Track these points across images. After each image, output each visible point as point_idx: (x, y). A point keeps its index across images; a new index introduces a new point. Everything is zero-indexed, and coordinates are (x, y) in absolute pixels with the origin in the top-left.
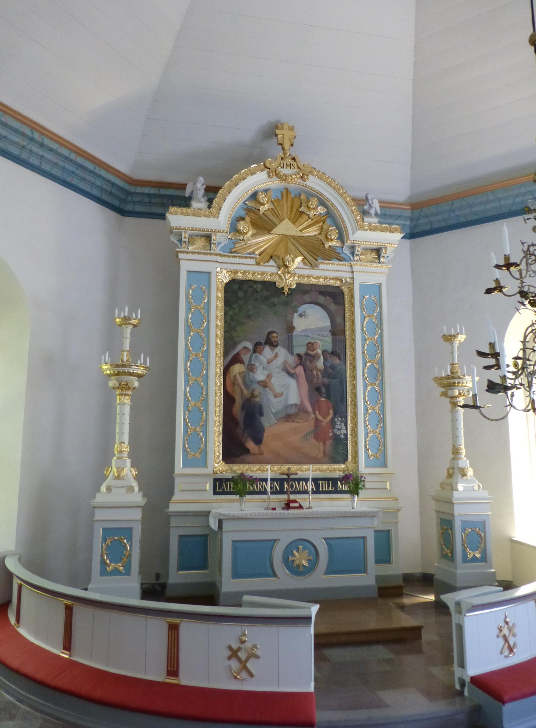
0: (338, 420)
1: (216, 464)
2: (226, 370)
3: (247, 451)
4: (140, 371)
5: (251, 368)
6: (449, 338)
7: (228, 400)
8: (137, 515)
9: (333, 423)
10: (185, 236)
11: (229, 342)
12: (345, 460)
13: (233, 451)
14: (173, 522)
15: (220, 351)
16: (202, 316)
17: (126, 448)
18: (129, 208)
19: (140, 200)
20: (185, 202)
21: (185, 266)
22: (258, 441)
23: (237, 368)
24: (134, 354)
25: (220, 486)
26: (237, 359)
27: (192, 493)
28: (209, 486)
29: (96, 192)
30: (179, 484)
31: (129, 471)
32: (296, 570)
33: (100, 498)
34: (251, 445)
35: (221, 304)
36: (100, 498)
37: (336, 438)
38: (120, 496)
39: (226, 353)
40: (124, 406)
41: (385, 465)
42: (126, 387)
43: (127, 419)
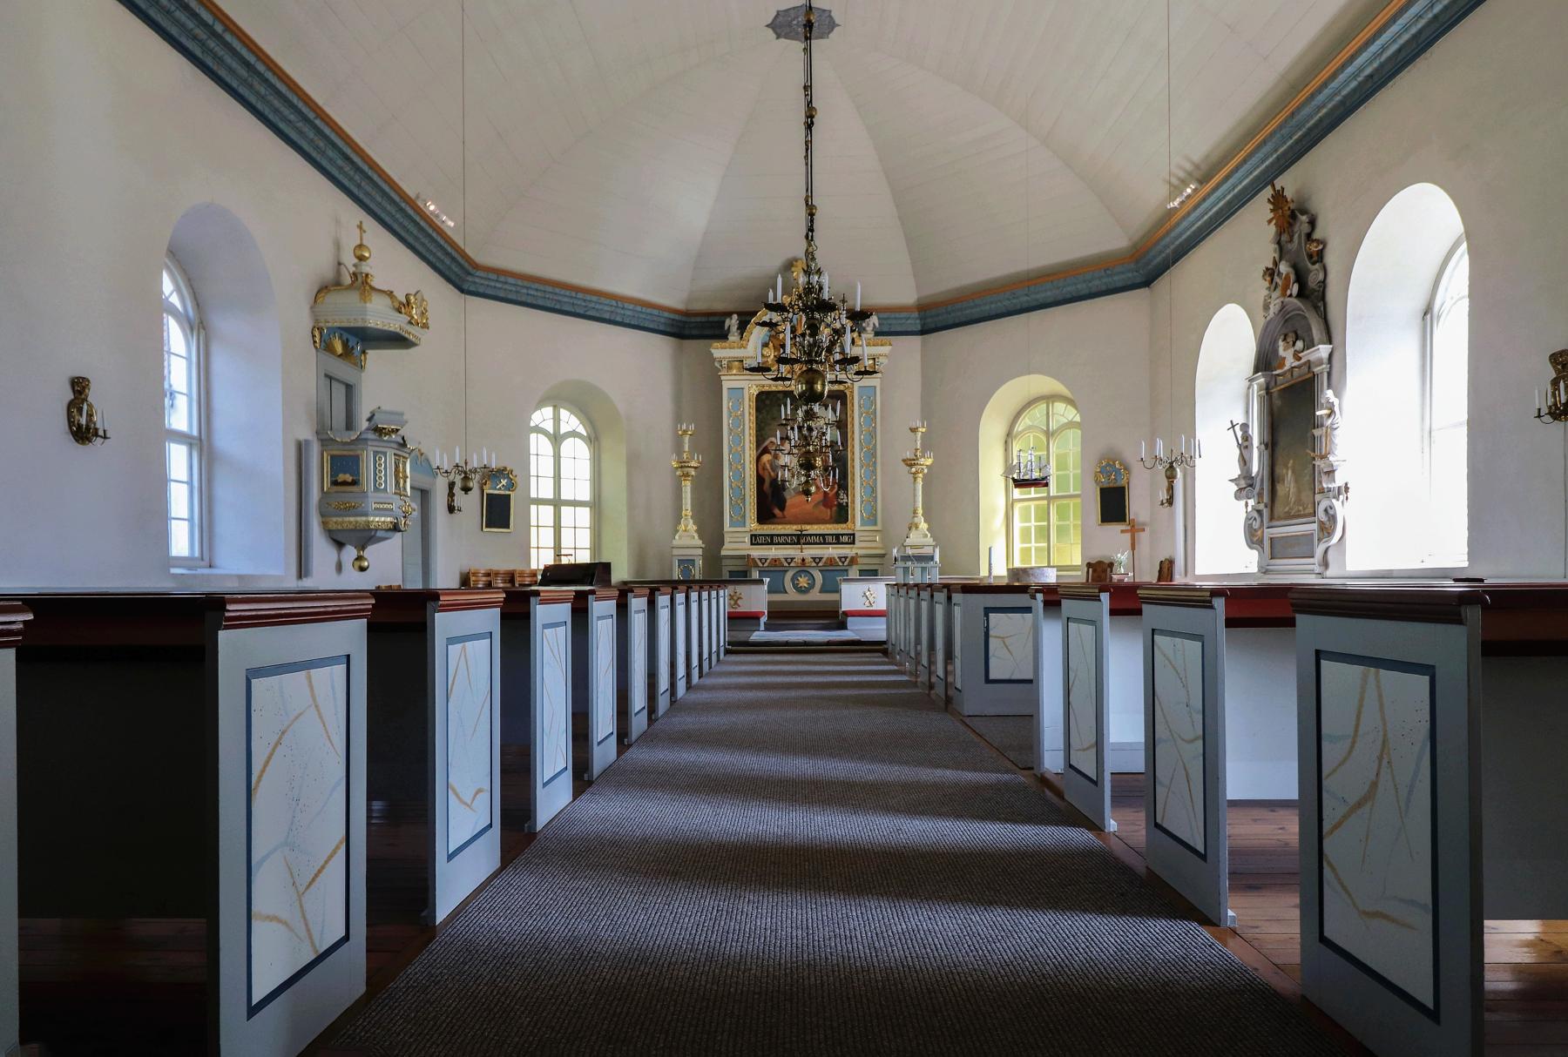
0: (842, 495)
1: (752, 525)
2: (758, 459)
3: (774, 516)
4: (693, 464)
5: (776, 457)
6: (914, 430)
7: (760, 480)
8: (700, 552)
9: (837, 494)
10: (724, 362)
11: (760, 438)
12: (846, 521)
13: (764, 516)
14: (725, 562)
15: (754, 446)
16: (739, 420)
17: (689, 513)
18: (687, 332)
19: (695, 327)
20: (723, 336)
21: (726, 385)
22: (782, 509)
23: (766, 458)
24: (691, 452)
25: (755, 540)
26: (766, 451)
27: (737, 543)
28: (747, 539)
29: (662, 328)
30: (727, 539)
31: (692, 527)
32: (800, 590)
33: (677, 541)
34: (777, 511)
35: (753, 412)
36: (675, 543)
37: (840, 505)
38: (687, 542)
39: (758, 444)
40: (687, 487)
41: (875, 524)
42: (687, 475)
43: (689, 495)
